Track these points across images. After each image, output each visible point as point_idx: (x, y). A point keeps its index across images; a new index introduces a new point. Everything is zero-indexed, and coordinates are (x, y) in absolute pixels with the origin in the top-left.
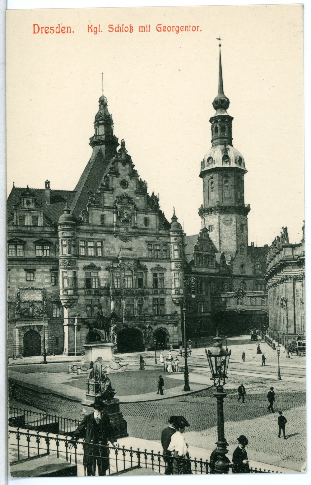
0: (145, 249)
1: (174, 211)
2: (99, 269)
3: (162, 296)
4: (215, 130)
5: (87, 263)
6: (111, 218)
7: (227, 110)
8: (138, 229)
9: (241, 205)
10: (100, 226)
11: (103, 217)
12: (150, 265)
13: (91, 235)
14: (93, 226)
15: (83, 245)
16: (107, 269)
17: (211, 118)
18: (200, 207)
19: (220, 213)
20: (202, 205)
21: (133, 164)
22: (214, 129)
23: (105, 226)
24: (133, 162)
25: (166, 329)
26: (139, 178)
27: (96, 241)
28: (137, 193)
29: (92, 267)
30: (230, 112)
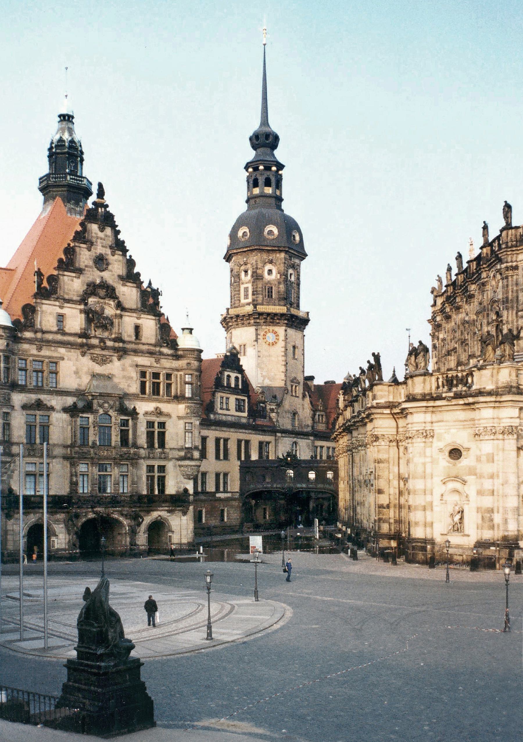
0: (135, 379)
2: (52, 409)
6: (75, 321)
7: (276, 152)
8: (124, 342)
9: (294, 311)
10: (56, 333)
11: (61, 318)
12: (144, 407)
14: (44, 332)
15: (24, 366)
16: (65, 410)
17: (248, 163)
18: (224, 312)
19: (257, 324)
21: (117, 229)
22: (251, 182)
23: (64, 334)
24: (117, 226)
25: (166, 520)
26: (128, 254)
27: (47, 360)
30: (280, 154)
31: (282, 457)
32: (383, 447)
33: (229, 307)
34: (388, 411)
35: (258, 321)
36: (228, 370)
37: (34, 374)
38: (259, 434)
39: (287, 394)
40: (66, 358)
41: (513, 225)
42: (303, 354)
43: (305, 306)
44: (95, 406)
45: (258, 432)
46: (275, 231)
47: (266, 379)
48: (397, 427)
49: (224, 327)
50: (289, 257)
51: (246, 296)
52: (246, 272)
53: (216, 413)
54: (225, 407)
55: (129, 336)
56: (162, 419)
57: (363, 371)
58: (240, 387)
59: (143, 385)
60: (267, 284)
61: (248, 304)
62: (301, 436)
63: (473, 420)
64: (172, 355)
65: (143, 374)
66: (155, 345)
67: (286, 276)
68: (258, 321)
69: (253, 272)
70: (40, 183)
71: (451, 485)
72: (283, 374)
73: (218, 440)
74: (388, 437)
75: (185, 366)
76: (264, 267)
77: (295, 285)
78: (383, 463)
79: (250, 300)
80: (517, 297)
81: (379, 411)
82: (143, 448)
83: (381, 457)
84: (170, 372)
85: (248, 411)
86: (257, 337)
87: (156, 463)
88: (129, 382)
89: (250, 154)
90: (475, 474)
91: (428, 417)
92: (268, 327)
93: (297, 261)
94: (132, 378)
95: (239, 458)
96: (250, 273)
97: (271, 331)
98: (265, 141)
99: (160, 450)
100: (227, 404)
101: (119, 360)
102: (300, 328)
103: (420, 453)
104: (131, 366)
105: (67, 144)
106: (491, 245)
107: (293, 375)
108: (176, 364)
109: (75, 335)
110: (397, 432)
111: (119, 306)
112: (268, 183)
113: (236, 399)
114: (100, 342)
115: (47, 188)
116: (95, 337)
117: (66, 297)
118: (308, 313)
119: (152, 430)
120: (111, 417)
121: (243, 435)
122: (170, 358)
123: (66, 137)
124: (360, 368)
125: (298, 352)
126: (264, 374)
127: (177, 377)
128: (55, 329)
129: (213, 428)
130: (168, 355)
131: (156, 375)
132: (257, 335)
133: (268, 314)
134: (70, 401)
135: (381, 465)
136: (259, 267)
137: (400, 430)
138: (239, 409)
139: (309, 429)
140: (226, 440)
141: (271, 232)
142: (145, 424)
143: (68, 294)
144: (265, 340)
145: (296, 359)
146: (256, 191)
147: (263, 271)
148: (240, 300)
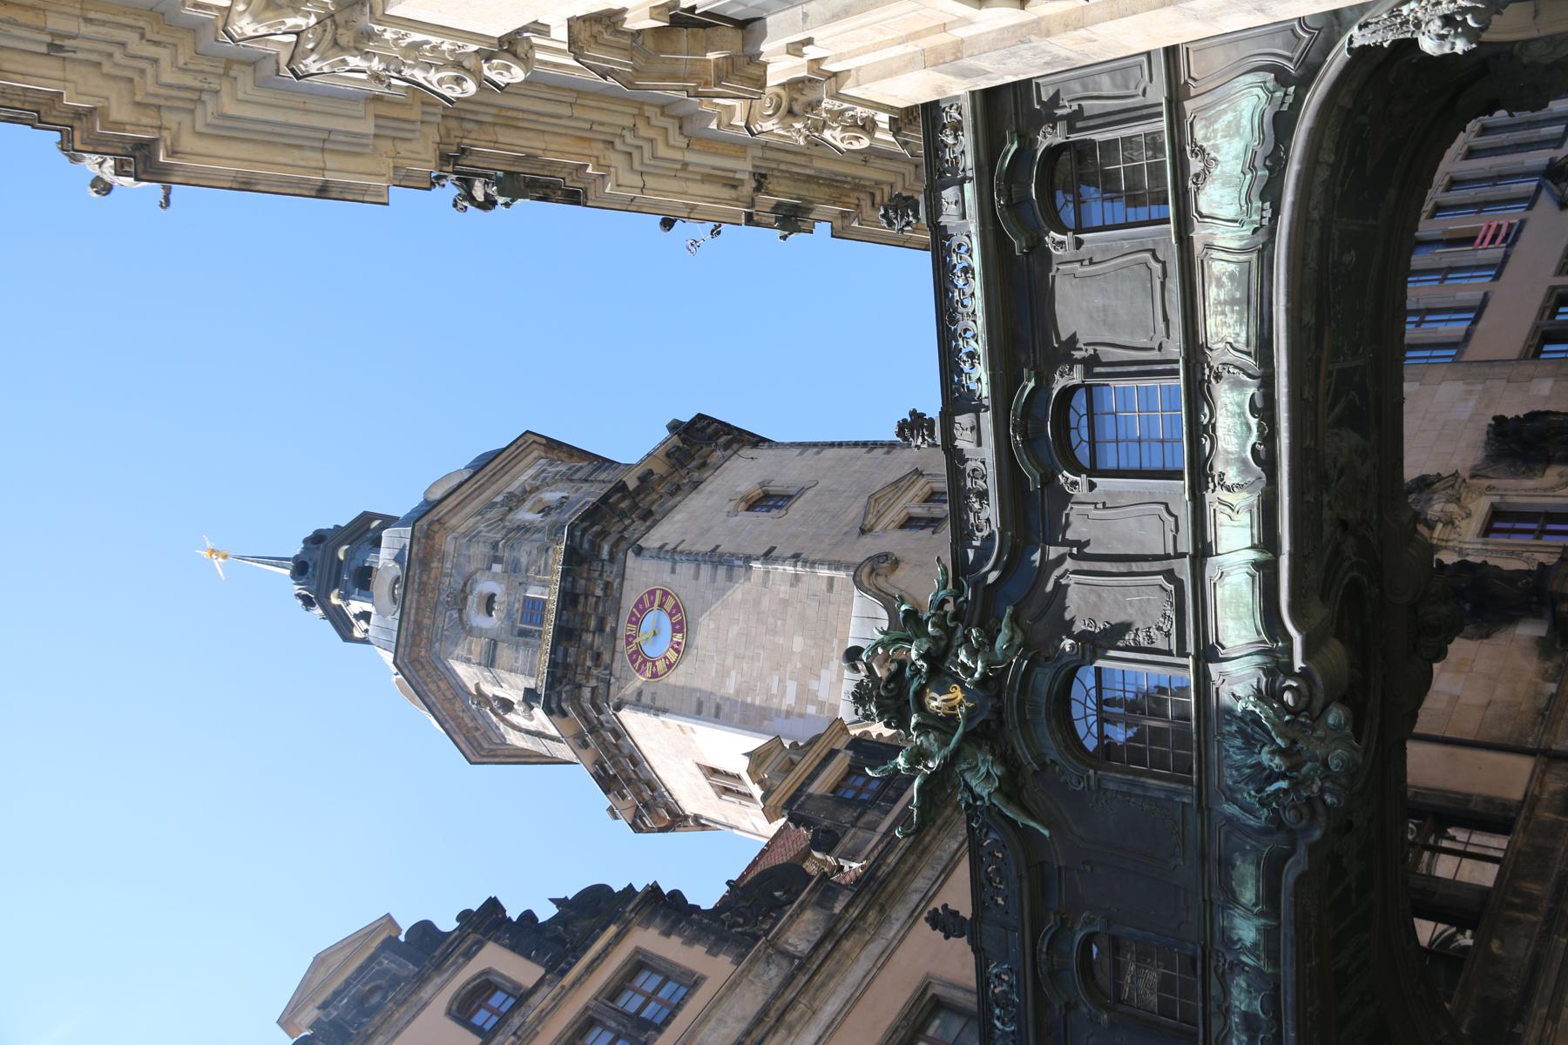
35: (587, 693)
39: (896, 563)
47: (814, 685)
50: (479, 513)
52: (507, 705)
60: (513, 626)
68: (587, 693)
77: (586, 486)
92: (621, 644)
96: (501, 693)
102: (704, 465)
132: (638, 704)
136: (465, 654)
144: (661, 665)
145: (802, 491)
147: (481, 633)
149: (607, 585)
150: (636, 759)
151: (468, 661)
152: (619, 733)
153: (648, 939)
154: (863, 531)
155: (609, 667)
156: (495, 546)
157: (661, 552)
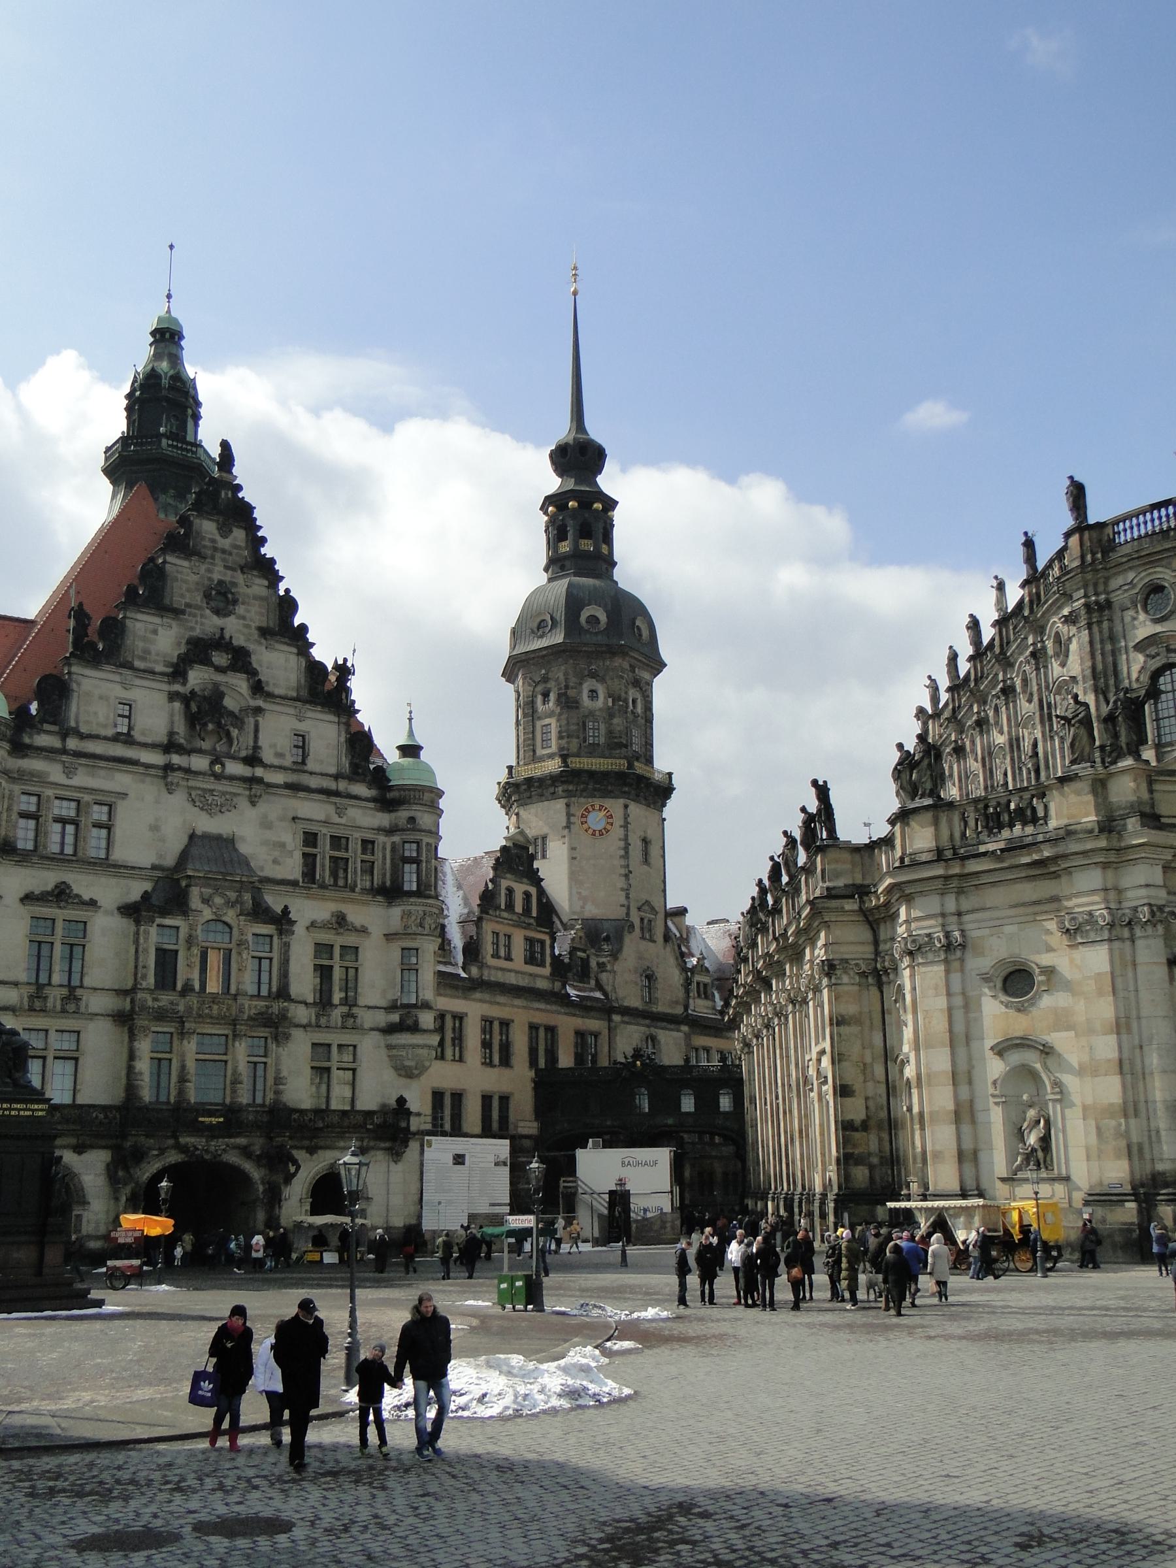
1: (410, 719)
3: (347, 1038)
4: (557, 532)
5: (44, 879)
6: (156, 714)
9: (640, 768)
12: (308, 910)
13: (69, 771)
15: (33, 808)
18: (503, 776)
19: (569, 794)
20: (510, 768)
27: (87, 798)
28: (264, 632)
29: (61, 894)
31: (623, 1060)
32: (846, 988)
33: (514, 764)
34: (851, 905)
35: (571, 787)
36: (508, 876)
37: (57, 827)
38: (574, 1015)
40: (132, 795)
41: (1092, 520)
42: (663, 857)
43: (664, 760)
44: (195, 902)
45: (572, 1010)
46: (603, 617)
48: (876, 942)
49: (503, 806)
50: (631, 666)
51: (546, 742)
52: (546, 695)
53: (482, 966)
54: (502, 953)
55: (280, 755)
56: (350, 940)
57: (791, 842)
58: (534, 914)
59: (309, 861)
60: (586, 717)
61: (551, 756)
62: (664, 1024)
63: (1055, 899)
64: (373, 800)
65: (310, 839)
66: (337, 777)
67: (626, 701)
68: (571, 787)
69: (559, 695)
70: (106, 459)
71: (1016, 1058)
72: (623, 894)
73: (487, 1022)
74: (857, 965)
75: (402, 822)
76: (581, 684)
77: (643, 721)
78: (849, 1024)
79: (554, 748)
80: (1115, 665)
81: (834, 903)
82: (306, 1004)
83: (844, 1012)
84: (369, 836)
85: (551, 964)
86: (568, 819)
87: (334, 1038)
88: (277, 854)
89: (553, 483)
90: (1069, 1027)
91: (951, 904)
93: (646, 675)
94: (282, 845)
95: (533, 1062)
96: (552, 697)
97: (597, 807)
98: (579, 458)
99: (345, 1009)
100: (508, 946)
101: (253, 804)
102: (654, 803)
103: (936, 988)
104: (282, 819)
105: (165, 382)
106: (1044, 574)
107: (644, 897)
108: (384, 819)
109: (153, 746)
110: (877, 953)
111: (258, 688)
112: (585, 532)
113: (527, 939)
114: (212, 763)
115: (123, 465)
116: (200, 751)
117: (138, 664)
118: (670, 774)
119: (326, 962)
120: (230, 927)
121: (543, 1014)
122: (371, 805)
123: (164, 366)
124: (785, 833)
125: (654, 851)
126: (584, 893)
127: (384, 848)
128: (110, 732)
129: (478, 995)
130: (367, 800)
131: (337, 842)
132: (569, 815)
133: (592, 774)
134: (136, 890)
135: (843, 1029)
136: (571, 684)
137: (882, 947)
138: (531, 960)
139: (679, 1010)
140: (505, 1024)
141: (593, 620)
142: (310, 950)
143: (143, 659)
144: (585, 826)
146: (565, 547)
147: (580, 692)
148: (534, 751)
149: (611, 792)
150: (542, 797)
151: (567, 687)
152: (554, 796)
153: (548, 942)
154: (639, 909)
155: (581, 796)
156: (619, 699)
157: (626, 816)
